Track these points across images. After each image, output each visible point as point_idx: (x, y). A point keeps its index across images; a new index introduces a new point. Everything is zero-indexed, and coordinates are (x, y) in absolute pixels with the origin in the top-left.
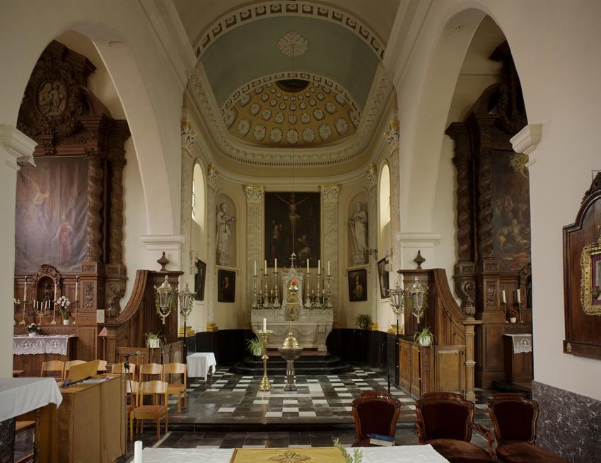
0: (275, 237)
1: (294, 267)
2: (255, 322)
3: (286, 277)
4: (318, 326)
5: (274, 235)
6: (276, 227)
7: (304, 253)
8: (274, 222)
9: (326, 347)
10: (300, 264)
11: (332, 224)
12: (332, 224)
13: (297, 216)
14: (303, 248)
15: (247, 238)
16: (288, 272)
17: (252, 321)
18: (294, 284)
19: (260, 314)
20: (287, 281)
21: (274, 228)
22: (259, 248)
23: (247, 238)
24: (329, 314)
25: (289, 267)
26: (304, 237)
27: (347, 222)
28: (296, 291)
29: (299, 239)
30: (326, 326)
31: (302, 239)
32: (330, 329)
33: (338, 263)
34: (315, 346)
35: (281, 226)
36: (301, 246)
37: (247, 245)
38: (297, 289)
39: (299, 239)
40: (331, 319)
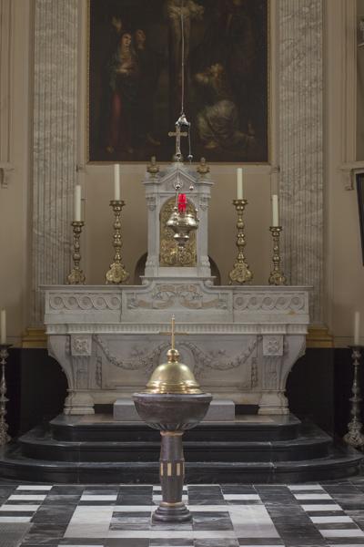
0: (123, 70)
1: (185, 160)
2: (52, 325)
3: (161, 190)
4: (260, 337)
5: (118, 64)
6: (127, 40)
7: (217, 119)
8: (119, 25)
9: (285, 401)
10: (202, 150)
11: (304, 31)
12: (304, 31)
13: (194, 8)
14: (211, 103)
15: (32, 72)
16: (163, 175)
17: (47, 321)
18: (183, 206)
19: (72, 300)
20: (159, 203)
21: (119, 42)
22: (72, 101)
23: (32, 72)
24: (296, 301)
25: (168, 158)
26: (216, 68)
27: (352, 25)
28: (190, 229)
29: (200, 77)
30: (284, 336)
31: (212, 74)
32: (297, 348)
33: (325, 150)
34: (249, 399)
35: (141, 36)
36: (206, 97)
37: (32, 94)
38: (191, 222)
39: (200, 77)
40: (303, 319)
